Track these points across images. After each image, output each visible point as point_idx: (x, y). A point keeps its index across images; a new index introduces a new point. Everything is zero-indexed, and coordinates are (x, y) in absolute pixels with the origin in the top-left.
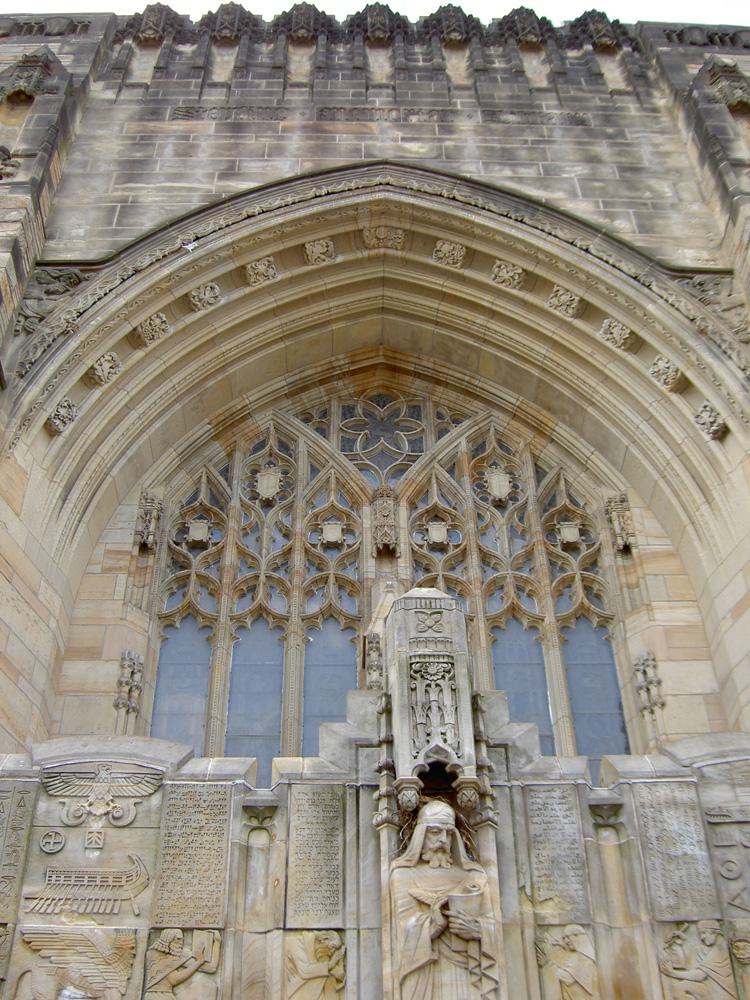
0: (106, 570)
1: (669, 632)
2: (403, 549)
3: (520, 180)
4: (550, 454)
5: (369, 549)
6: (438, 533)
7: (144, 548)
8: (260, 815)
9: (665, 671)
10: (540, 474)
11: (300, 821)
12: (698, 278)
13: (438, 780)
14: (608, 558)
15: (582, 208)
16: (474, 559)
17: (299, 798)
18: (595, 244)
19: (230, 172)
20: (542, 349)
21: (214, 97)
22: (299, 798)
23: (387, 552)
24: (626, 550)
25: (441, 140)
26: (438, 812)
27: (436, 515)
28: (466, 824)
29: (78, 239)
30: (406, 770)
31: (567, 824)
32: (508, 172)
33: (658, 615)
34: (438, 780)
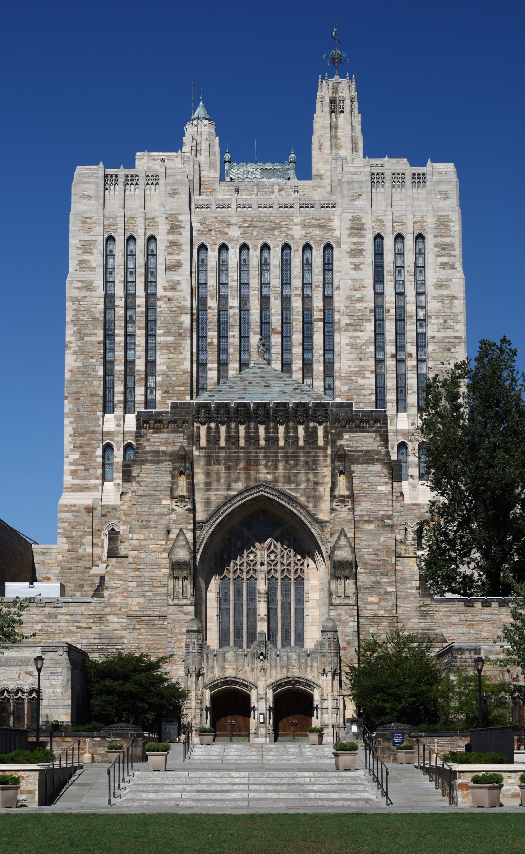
1: (312, 586)
2: (266, 563)
3: (290, 489)
5: (259, 563)
6: (273, 557)
7: (216, 565)
8: (246, 655)
11: (249, 656)
13: (262, 654)
15: (302, 499)
16: (279, 565)
17: (249, 654)
18: (304, 512)
19: (229, 488)
21: (222, 454)
22: (249, 654)
23: (262, 564)
25: (275, 473)
26: (262, 657)
27: (273, 552)
28: (264, 658)
29: (200, 516)
31: (274, 656)
32: (288, 487)
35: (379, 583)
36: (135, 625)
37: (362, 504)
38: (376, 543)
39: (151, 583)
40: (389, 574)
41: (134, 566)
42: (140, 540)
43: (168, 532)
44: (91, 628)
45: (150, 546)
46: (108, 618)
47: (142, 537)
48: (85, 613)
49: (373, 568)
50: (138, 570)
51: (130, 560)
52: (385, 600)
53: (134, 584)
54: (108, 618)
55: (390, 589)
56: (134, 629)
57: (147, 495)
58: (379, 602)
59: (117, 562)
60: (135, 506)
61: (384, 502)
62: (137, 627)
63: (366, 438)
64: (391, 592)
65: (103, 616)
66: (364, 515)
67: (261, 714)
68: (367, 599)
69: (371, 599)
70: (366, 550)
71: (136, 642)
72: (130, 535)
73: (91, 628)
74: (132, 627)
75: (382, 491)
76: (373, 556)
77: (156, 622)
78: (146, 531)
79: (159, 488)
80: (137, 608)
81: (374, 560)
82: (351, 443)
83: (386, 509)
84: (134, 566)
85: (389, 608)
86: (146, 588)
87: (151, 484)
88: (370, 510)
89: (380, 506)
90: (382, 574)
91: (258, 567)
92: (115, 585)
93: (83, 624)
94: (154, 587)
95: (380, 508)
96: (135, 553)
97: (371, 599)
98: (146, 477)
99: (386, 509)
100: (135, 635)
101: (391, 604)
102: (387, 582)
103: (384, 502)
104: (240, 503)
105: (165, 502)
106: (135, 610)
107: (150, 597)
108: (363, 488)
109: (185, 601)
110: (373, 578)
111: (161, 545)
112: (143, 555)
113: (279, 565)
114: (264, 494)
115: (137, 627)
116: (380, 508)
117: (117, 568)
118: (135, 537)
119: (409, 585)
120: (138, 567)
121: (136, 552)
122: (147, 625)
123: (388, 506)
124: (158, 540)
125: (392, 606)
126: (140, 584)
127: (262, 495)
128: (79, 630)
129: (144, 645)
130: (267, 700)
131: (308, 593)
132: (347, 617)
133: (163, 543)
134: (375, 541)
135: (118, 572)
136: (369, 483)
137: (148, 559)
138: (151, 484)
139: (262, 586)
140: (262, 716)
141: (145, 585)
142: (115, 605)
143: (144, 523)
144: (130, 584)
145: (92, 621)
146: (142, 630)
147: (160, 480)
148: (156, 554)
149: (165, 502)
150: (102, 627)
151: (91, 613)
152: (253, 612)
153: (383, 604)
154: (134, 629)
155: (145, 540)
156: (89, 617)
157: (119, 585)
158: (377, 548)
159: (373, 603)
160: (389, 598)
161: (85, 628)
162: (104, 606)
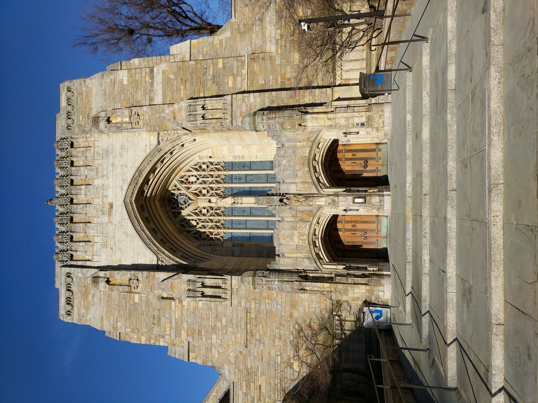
0: (216, 251)
1: (229, 152)
4: (186, 169)
7: (210, 245)
9: (237, 155)
10: (189, 171)
12: (160, 139)
14: (211, 160)
20: (167, 169)
23: (210, 201)
24: (210, 157)
26: (285, 201)
30: (280, 204)
33: (225, 154)
34: (281, 201)
35: (214, 76)
36: (257, 340)
37: (139, 99)
38: (175, 83)
39: (213, 319)
40: (205, 66)
41: (196, 336)
42: (171, 327)
43: (163, 298)
44: (260, 386)
45: (177, 317)
46: (249, 366)
47: (168, 325)
48: (244, 391)
49: (199, 84)
50: (200, 332)
51: (190, 339)
52: (231, 68)
53: (214, 337)
54: (249, 366)
55: (220, 65)
56: (259, 340)
57: (130, 317)
58: (233, 75)
59: (194, 352)
60: (140, 330)
61: (138, 77)
62: (258, 337)
63: (83, 100)
64: (223, 63)
65: (247, 371)
66: (150, 97)
67: (354, 202)
68: (230, 88)
69: (230, 84)
70: (182, 92)
71: (274, 340)
72: (166, 337)
73: (260, 386)
74: (257, 343)
75: (128, 80)
76: (188, 84)
77: (253, 316)
78: (163, 320)
79: (124, 304)
80: (238, 335)
81: (192, 84)
82: (87, 113)
83: (144, 75)
84: (196, 336)
85: (240, 64)
86: (219, 324)
87: (119, 312)
88: (145, 91)
89: (141, 81)
90: (205, 74)
91: (212, 205)
92: (217, 356)
93: (256, 394)
94: (217, 316)
95: (143, 81)
96: (184, 333)
97: (230, 84)
98: (114, 317)
99: (144, 75)
100: (266, 340)
101: (235, 63)
102: (214, 69)
103: (138, 77)
104: (142, 223)
105: (137, 300)
106: (241, 337)
107: (227, 321)
108: (124, 99)
109: (228, 286)
110: (209, 83)
111: (176, 306)
112: (185, 325)
113: (212, 186)
114: (134, 199)
115: (258, 337)
116: (143, 81)
117: (199, 352)
118: (168, 332)
119: (218, 46)
120: (197, 332)
121: (183, 332)
122: (256, 326)
123: (141, 73)
124: (171, 309)
125: (238, 62)
126: (214, 329)
127: (135, 201)
128: (262, 399)
129: (277, 331)
130: (337, 195)
131: (235, 157)
132: (244, 105)
133: (173, 303)
134: (173, 84)
135: (203, 351)
136: (120, 93)
137: (189, 321)
138: (119, 312)
139: (228, 202)
140: (357, 200)
141: (215, 326)
142: (236, 357)
143: (155, 322)
144: (214, 341)
145: (252, 384)
146: (261, 332)
147: (116, 303)
148: (185, 312)
149: (137, 300)
150: (259, 373)
151: (244, 384)
152: (251, 212)
153: (235, 70)
154: (259, 340)
155: (171, 323)
156: (248, 386)
157: (217, 352)
158: (180, 81)
159: (234, 81)
160: (230, 65)
161: (260, 392)
162: (237, 370)
